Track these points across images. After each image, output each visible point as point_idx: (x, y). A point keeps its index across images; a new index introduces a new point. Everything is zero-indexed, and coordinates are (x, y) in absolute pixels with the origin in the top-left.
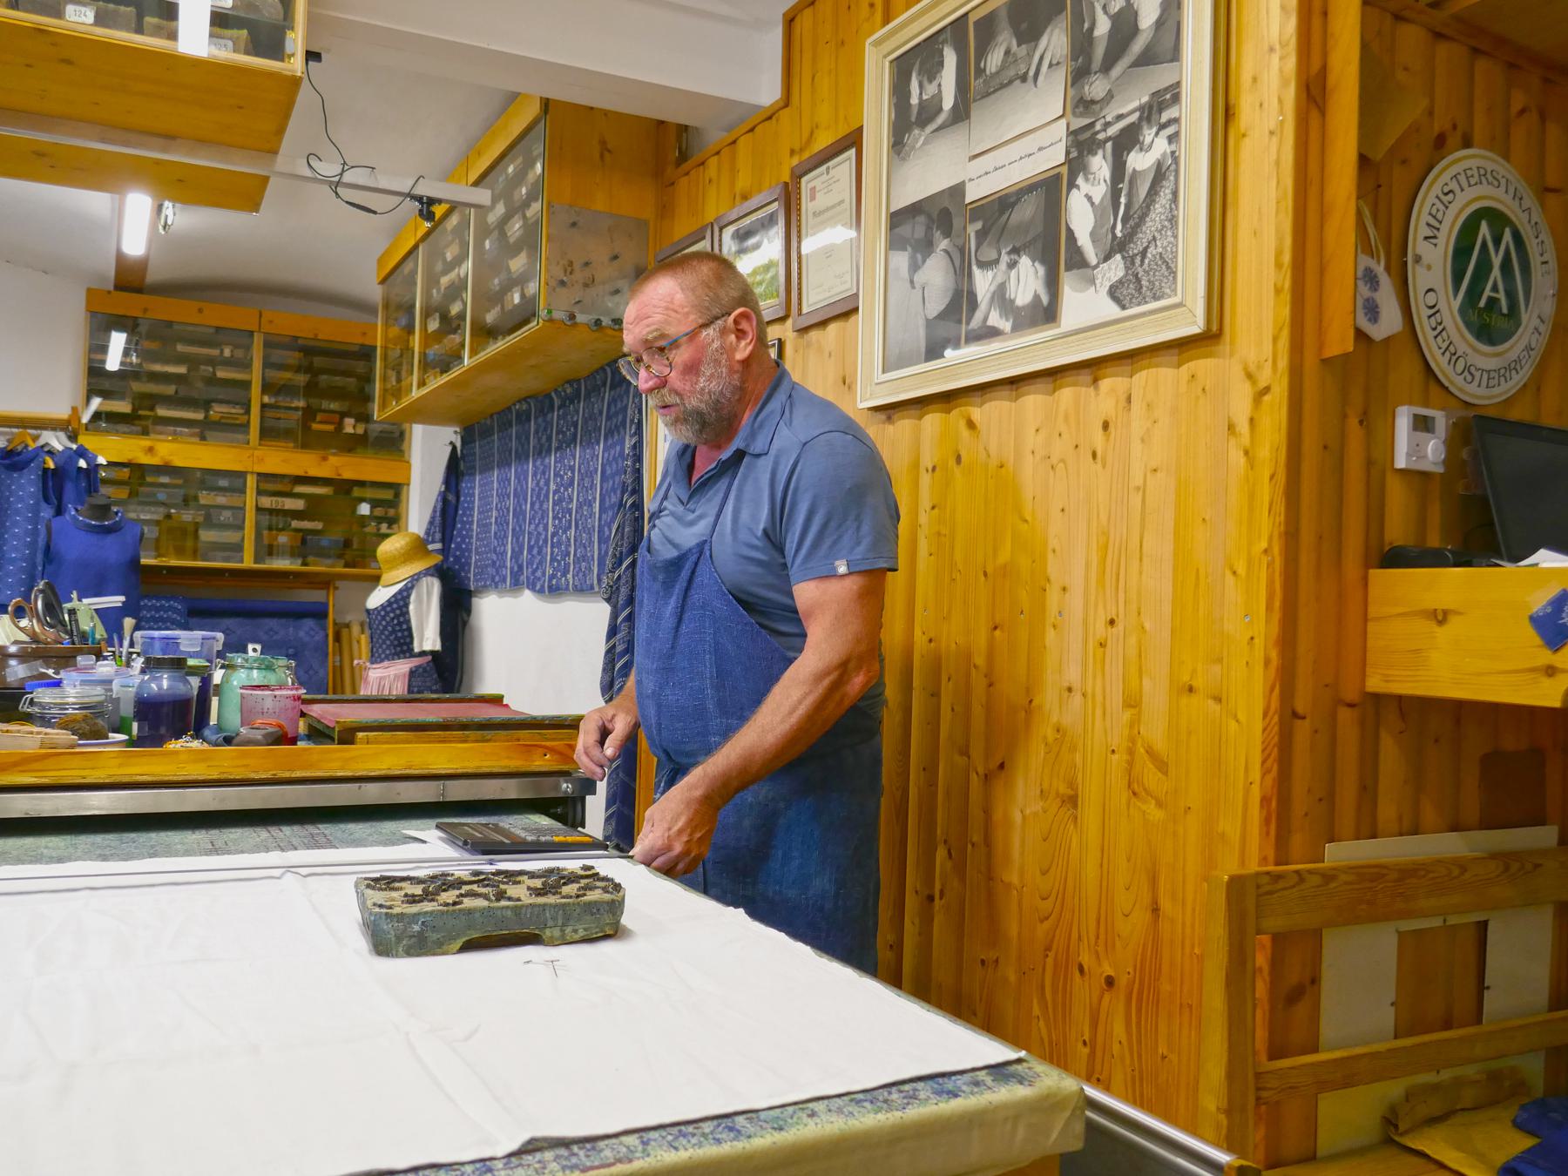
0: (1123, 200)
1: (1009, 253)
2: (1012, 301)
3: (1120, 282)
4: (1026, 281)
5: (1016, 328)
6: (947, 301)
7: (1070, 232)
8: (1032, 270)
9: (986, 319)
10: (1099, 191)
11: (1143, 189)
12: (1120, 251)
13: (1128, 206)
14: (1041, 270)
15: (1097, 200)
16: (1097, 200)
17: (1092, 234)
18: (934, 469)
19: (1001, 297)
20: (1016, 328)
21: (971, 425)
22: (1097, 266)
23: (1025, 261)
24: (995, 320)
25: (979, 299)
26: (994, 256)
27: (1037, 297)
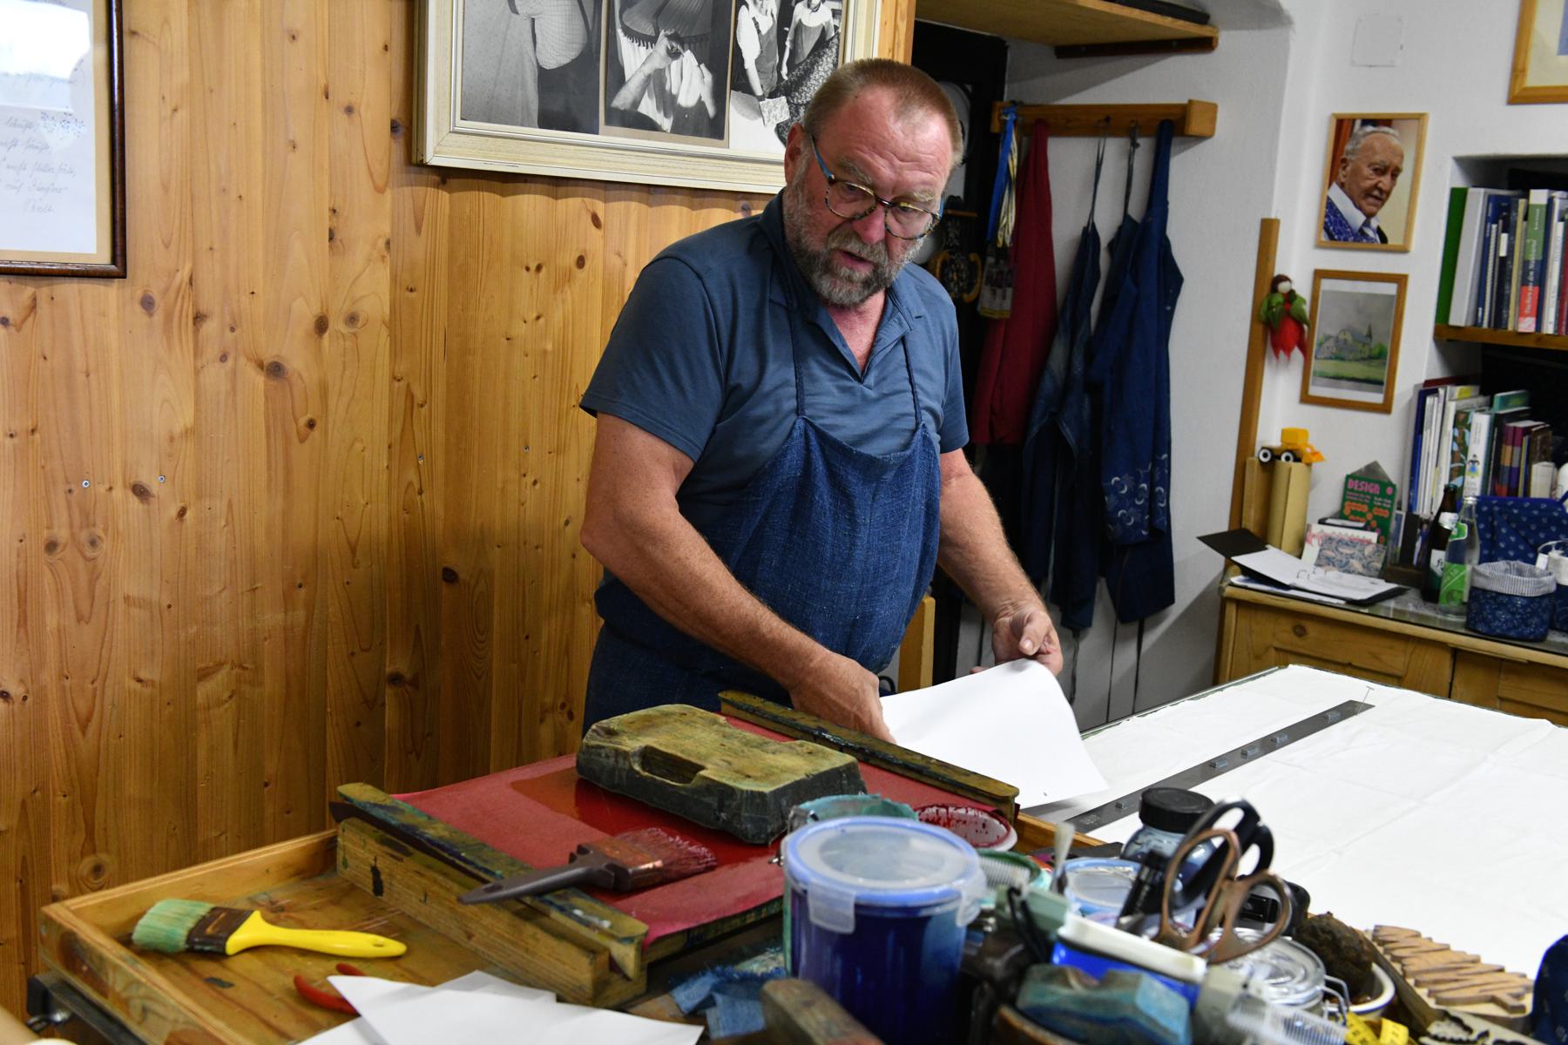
0: (788, 44)
1: (670, 38)
2: (674, 98)
3: (786, 123)
4: (691, 82)
5: (677, 129)
6: (573, 54)
7: (738, 52)
8: (697, 71)
9: (636, 103)
10: (767, 23)
11: (808, 45)
12: (787, 94)
13: (793, 53)
14: (708, 77)
15: (764, 32)
16: (764, 32)
17: (757, 62)
18: (539, 268)
19: (656, 82)
20: (677, 129)
21: (596, 221)
22: (761, 98)
23: (688, 57)
24: (648, 107)
25: (628, 75)
26: (650, 31)
27: (700, 103)
